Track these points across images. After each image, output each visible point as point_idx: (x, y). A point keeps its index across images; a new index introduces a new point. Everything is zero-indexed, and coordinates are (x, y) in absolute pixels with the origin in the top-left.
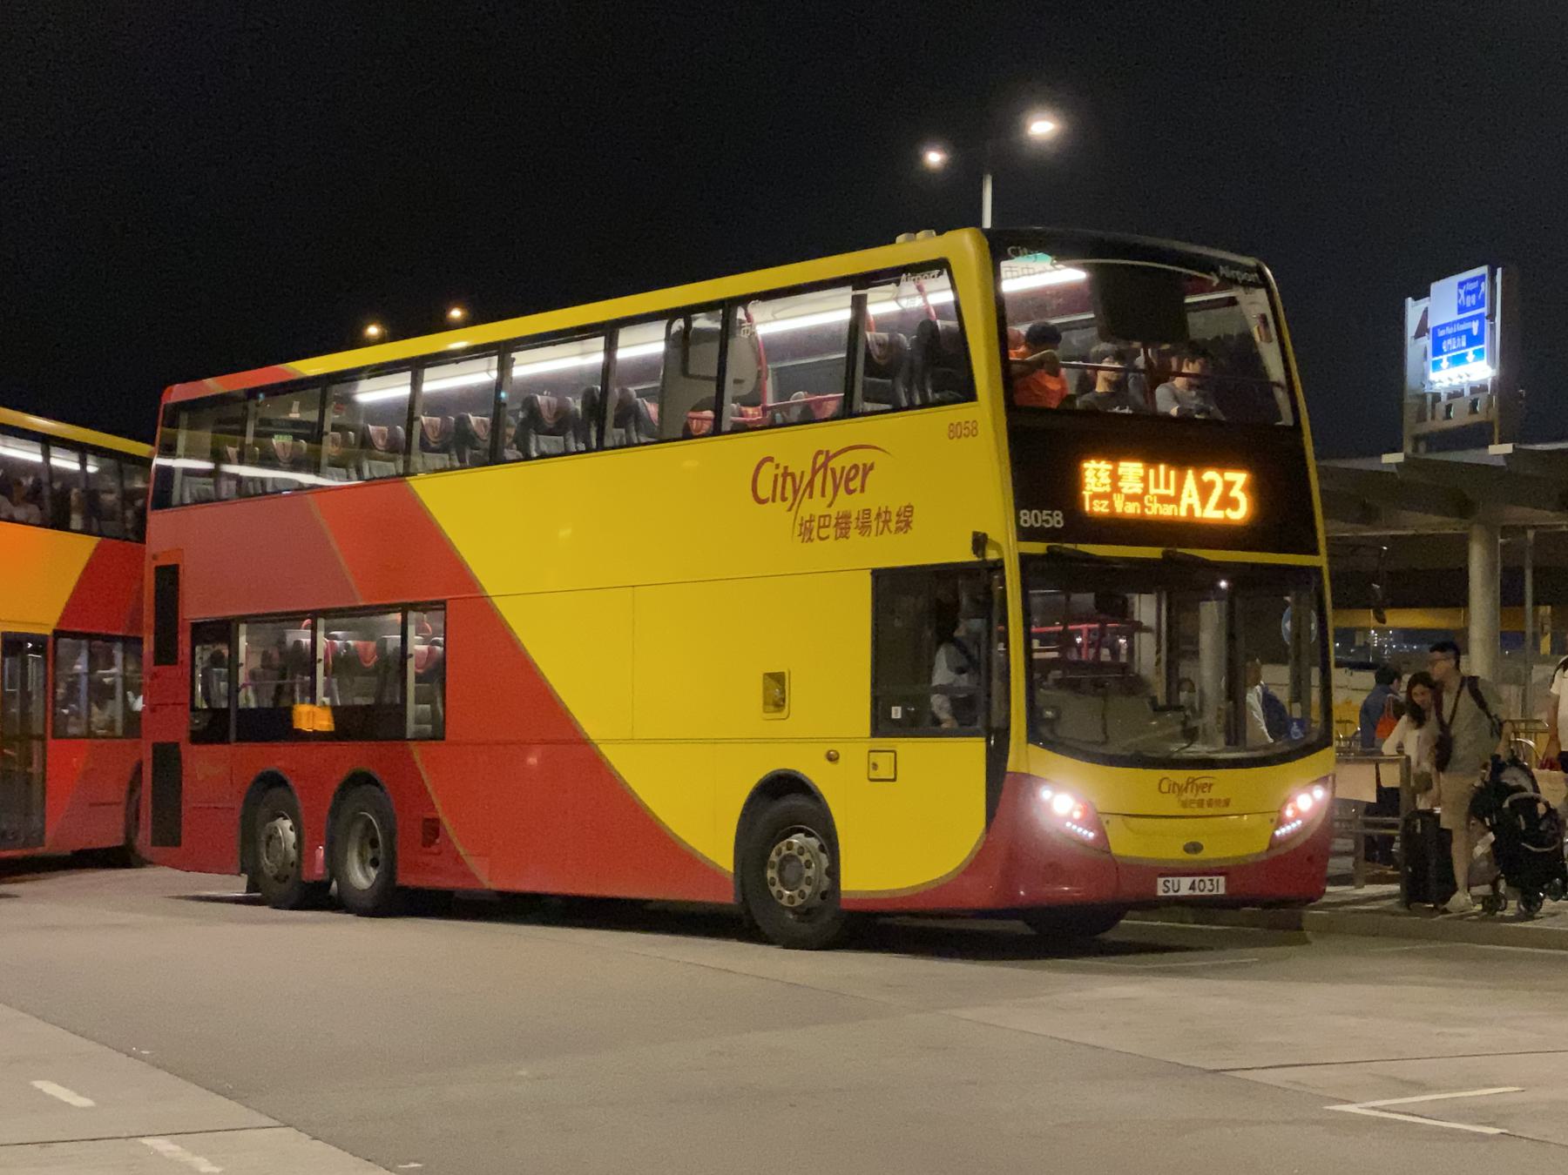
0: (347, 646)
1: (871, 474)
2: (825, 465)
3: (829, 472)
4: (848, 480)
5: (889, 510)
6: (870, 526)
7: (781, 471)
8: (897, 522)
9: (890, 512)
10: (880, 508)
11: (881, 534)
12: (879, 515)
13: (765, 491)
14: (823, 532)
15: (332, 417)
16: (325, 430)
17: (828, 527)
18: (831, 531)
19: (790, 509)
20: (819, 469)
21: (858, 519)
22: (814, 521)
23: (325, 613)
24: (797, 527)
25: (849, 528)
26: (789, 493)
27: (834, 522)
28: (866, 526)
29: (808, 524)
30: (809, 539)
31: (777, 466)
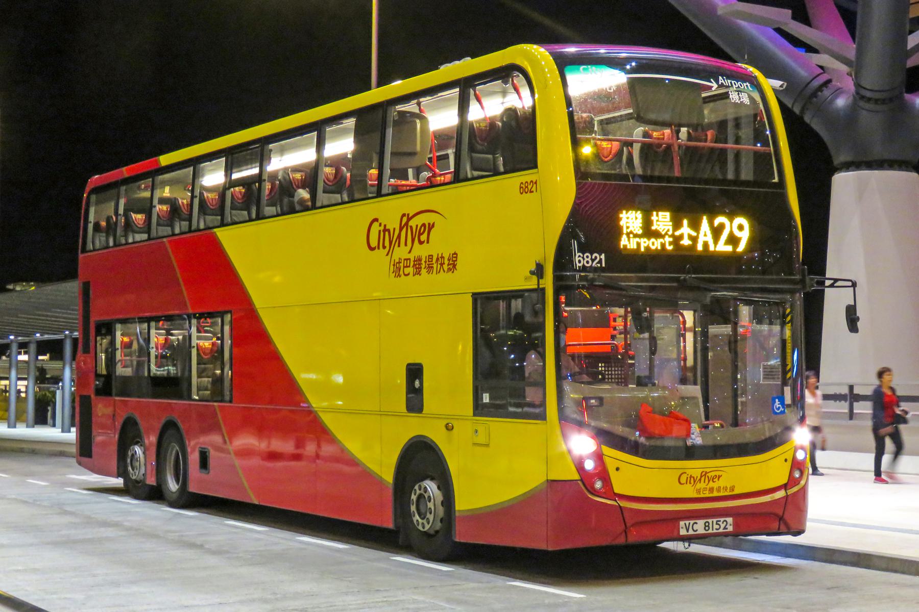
0: (178, 339)
1: (433, 229)
2: (407, 224)
3: (409, 228)
4: (420, 234)
5: (443, 256)
6: (432, 267)
7: (382, 228)
8: (448, 265)
9: (444, 257)
10: (438, 254)
11: (439, 272)
12: (438, 259)
13: (374, 243)
14: (407, 271)
15: (158, 194)
16: (153, 205)
17: (409, 266)
18: (410, 270)
19: (387, 255)
20: (404, 226)
21: (426, 262)
22: (401, 262)
23: (157, 319)
24: (392, 267)
25: (421, 268)
26: (387, 244)
27: (412, 264)
28: (430, 267)
29: (398, 266)
30: (399, 274)
31: (380, 225)
